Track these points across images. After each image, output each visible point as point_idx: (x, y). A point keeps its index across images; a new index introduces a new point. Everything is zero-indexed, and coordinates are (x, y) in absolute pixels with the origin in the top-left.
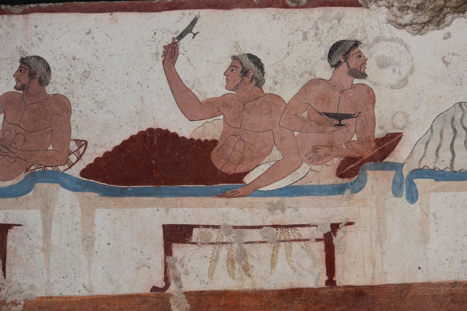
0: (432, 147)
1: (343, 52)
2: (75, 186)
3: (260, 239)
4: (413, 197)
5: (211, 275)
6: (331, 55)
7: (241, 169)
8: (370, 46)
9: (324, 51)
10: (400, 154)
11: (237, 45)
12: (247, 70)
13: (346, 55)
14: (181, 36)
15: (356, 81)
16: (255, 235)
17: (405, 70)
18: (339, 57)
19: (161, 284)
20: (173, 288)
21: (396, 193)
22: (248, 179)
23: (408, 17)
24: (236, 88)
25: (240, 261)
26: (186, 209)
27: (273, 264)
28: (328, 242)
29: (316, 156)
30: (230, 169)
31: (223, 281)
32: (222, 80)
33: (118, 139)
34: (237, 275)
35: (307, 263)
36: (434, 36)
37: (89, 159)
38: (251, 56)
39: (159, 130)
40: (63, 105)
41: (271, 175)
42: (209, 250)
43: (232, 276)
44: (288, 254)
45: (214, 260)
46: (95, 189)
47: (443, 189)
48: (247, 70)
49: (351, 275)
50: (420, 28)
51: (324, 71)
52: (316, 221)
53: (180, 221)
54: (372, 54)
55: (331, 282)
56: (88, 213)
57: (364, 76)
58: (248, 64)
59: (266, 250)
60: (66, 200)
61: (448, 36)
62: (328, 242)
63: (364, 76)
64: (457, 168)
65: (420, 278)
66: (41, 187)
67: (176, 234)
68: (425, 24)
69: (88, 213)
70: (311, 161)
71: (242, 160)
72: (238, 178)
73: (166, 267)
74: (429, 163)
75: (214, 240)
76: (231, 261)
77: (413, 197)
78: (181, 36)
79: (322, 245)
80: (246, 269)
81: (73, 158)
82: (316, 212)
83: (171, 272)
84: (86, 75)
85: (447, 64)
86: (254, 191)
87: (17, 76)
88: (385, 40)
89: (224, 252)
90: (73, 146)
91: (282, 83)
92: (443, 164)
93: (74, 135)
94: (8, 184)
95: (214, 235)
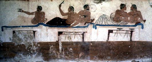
0: (99, 21)
1: (86, 7)
2: (45, 25)
3: (73, 34)
4: (96, 28)
5: (65, 39)
6: (84, 7)
7: (70, 23)
8: (90, 6)
9: (83, 6)
10: (94, 22)
11: (70, 5)
12: (71, 8)
13: (86, 7)
14: (62, 3)
15: (88, 11)
16: (72, 33)
17: (95, 9)
18: (85, 7)
19: (58, 40)
20: (59, 41)
21: (93, 28)
22: (72, 25)
23: (96, 1)
24: (70, 11)
25: (70, 38)
26: (61, 30)
27: (75, 38)
28: (83, 35)
29: (81, 22)
30: (69, 23)
31: (67, 40)
32: (68, 10)
33: (52, 19)
34: (69, 39)
35: (80, 38)
36: (100, 4)
37: (47, 22)
38: (72, 7)
39: (58, 17)
40: (44, 13)
41: (75, 24)
42: (65, 35)
43: (68, 39)
44: (77, 36)
45: (66, 37)
46: (48, 26)
47: (100, 27)
48: (71, 8)
49: (86, 40)
50: (98, 3)
51: (83, 9)
52: (81, 32)
53: (61, 31)
54: (90, 7)
55: (83, 41)
56: (47, 30)
57: (89, 10)
58: (71, 7)
59: (74, 36)
60: (44, 27)
61: (102, 4)
62: (83, 35)
63: (89, 10)
64: (103, 24)
65: (97, 41)
66: (41, 25)
67: (60, 33)
68: (98, 3)
69: (47, 30)
70: (80, 23)
71: (70, 22)
72: (70, 25)
73: (58, 38)
74: (99, 23)
75: (66, 34)
76: (68, 37)
77: (96, 28)
78: (62, 3)
79: (82, 35)
80: (71, 38)
81: (45, 21)
82: (81, 30)
83: (59, 39)
84: (48, 9)
85: (102, 9)
86: (72, 27)
87: (37, 9)
88: (92, 5)
89: (67, 36)
90: (45, 19)
91: (77, 11)
92: (101, 23)
93: (45, 18)
94: (34, 25)
95: (66, 33)
